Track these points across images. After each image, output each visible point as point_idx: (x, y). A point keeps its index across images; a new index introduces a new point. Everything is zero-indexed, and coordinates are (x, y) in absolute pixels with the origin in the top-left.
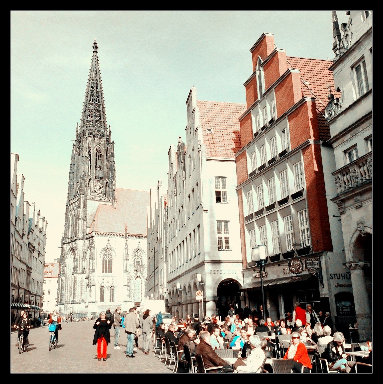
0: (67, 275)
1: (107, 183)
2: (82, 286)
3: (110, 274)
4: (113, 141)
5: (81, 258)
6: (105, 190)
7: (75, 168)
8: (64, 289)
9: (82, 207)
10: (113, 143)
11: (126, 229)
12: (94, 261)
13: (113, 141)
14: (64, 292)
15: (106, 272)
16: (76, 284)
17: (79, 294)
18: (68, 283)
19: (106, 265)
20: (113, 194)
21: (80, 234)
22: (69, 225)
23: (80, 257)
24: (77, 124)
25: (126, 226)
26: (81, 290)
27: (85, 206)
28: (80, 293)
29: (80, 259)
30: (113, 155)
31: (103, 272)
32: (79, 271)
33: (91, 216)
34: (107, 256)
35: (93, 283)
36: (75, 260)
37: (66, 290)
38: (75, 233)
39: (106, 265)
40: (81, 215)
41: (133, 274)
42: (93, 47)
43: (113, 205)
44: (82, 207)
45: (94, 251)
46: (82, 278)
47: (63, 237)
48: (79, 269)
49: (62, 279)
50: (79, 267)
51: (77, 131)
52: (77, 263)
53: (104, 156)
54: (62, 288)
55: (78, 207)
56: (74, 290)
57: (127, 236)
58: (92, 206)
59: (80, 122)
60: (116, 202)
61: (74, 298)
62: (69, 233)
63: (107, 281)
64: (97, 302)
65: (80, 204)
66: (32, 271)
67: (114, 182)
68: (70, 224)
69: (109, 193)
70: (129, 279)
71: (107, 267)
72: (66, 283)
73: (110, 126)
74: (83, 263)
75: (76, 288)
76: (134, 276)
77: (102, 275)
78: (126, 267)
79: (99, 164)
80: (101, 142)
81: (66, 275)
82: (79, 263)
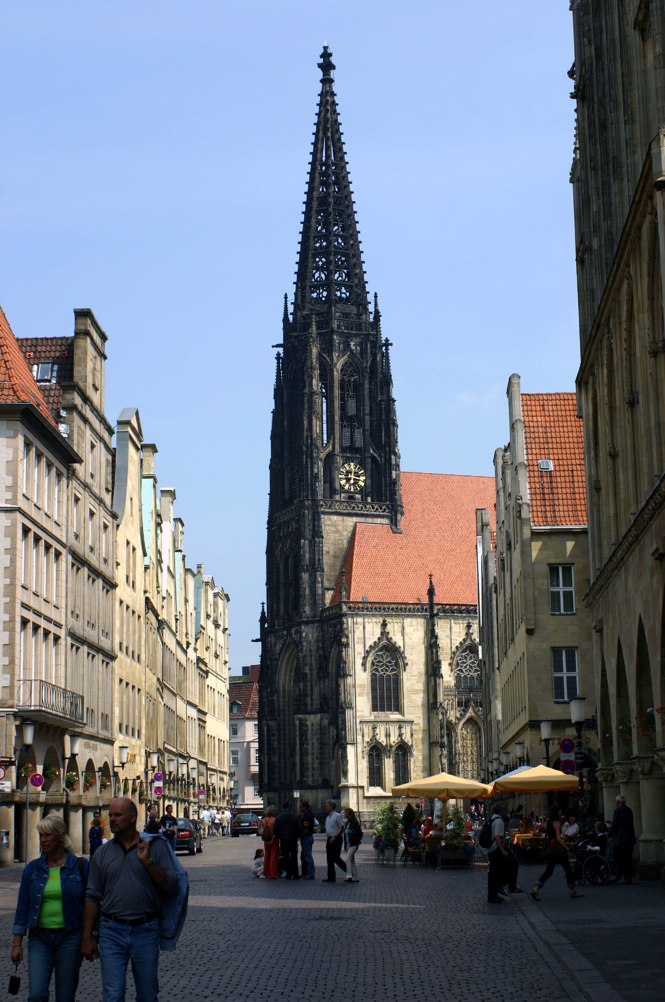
0: (282, 714)
2: (322, 744)
4: (387, 340)
5: (315, 672)
6: (369, 482)
7: (286, 423)
8: (276, 751)
9: (308, 533)
10: (387, 344)
11: (431, 592)
12: (349, 680)
13: (387, 340)
14: (275, 758)
15: (382, 710)
16: (306, 739)
17: (316, 766)
18: (284, 734)
19: (382, 689)
20: (393, 493)
22: (278, 582)
23: (311, 669)
24: (286, 297)
25: (431, 582)
26: (321, 753)
27: (317, 533)
28: (317, 761)
29: (311, 674)
30: (387, 381)
31: (374, 708)
32: (312, 704)
33: (334, 557)
34: (381, 666)
35: (349, 738)
36: (299, 676)
37: (280, 753)
38: (296, 603)
39: (382, 689)
40: (307, 556)
42: (320, 66)
43: (394, 522)
44: (308, 533)
45: (347, 655)
46: (320, 724)
47: (263, 613)
48: (312, 700)
49: (268, 725)
50: (312, 695)
52: (305, 686)
53: (363, 385)
54: (271, 749)
56: (301, 755)
57: (435, 612)
58: (335, 529)
59: (291, 290)
60: (402, 514)
61: (302, 776)
62: (278, 602)
64: (362, 787)
67: (393, 457)
68: (282, 581)
69: (383, 492)
71: (387, 695)
72: (279, 735)
73: (376, 296)
74: (322, 686)
75: (307, 749)
76: (456, 718)
77: (372, 718)
78: (435, 695)
80: (353, 348)
81: (279, 716)
82: (311, 685)
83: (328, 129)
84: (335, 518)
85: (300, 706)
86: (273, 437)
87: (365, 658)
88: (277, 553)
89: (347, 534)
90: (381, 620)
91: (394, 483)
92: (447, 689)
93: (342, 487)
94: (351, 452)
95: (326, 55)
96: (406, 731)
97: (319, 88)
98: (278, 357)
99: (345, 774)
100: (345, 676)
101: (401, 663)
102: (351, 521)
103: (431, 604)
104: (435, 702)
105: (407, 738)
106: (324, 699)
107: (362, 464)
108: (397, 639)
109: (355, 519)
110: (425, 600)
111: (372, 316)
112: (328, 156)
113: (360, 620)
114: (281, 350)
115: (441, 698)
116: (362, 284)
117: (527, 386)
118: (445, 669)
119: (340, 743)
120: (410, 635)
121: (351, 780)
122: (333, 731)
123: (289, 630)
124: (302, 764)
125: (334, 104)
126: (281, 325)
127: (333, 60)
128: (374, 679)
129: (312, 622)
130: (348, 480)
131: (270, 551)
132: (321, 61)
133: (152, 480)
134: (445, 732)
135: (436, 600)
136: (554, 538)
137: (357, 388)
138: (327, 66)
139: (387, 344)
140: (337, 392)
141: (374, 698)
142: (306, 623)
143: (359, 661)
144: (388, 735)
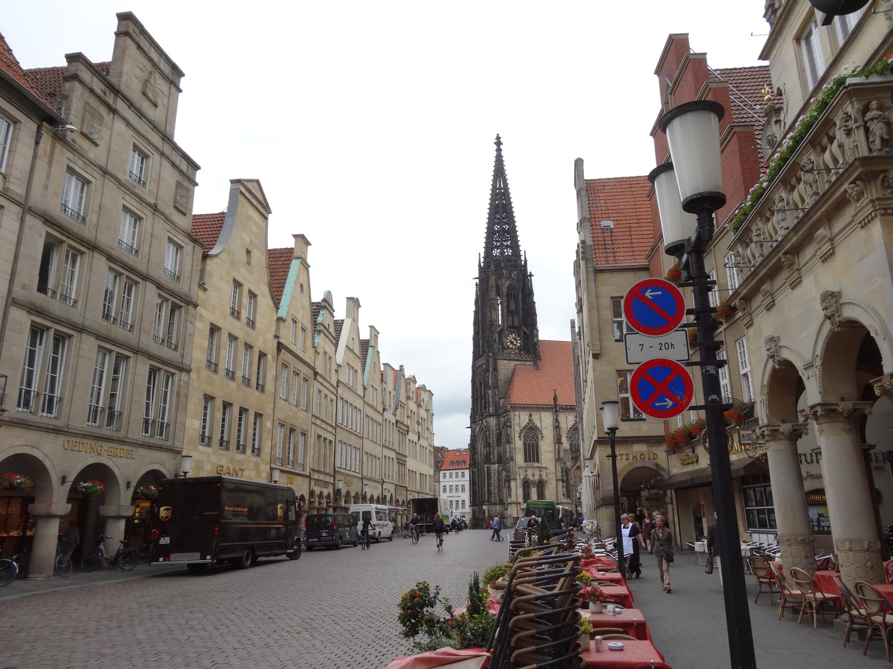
1: (525, 333)
2: (499, 480)
3: (536, 464)
10: (531, 275)
11: (555, 399)
12: (512, 446)
20: (536, 349)
21: (491, 409)
27: (495, 369)
30: (531, 293)
31: (526, 461)
35: (512, 477)
36: (488, 445)
41: (569, 464)
55: (487, 370)
58: (505, 367)
59: (482, 251)
63: (533, 475)
65: (488, 366)
66: (408, 459)
70: (566, 472)
71: (532, 454)
78: (559, 454)
79: (512, 307)
83: (499, 172)
84: (505, 362)
85: (488, 460)
88: (477, 381)
89: (511, 370)
90: (528, 413)
91: (536, 344)
92: (565, 450)
93: (508, 346)
94: (513, 328)
95: (498, 138)
96: (544, 473)
97: (495, 153)
98: (477, 285)
99: (510, 495)
101: (540, 436)
102: (513, 363)
103: (556, 406)
104: (559, 457)
105: (544, 477)
106: (500, 456)
107: (519, 335)
108: (538, 423)
109: (516, 362)
113: (517, 413)
114: (477, 281)
115: (562, 455)
117: (590, 174)
118: (564, 439)
119: (508, 480)
120: (544, 421)
121: (513, 499)
122: (504, 473)
123: (482, 420)
124: (488, 491)
127: (501, 140)
128: (525, 444)
129: (493, 416)
130: (512, 343)
131: (473, 381)
133: (299, 260)
134: (564, 473)
135: (558, 403)
136: (615, 274)
137: (516, 297)
138: (498, 143)
139: (531, 275)
140: (505, 299)
141: (525, 456)
142: (490, 416)
143: (517, 435)
144: (533, 475)
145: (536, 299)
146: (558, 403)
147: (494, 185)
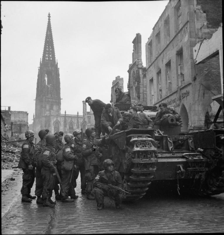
10: (59, 69)
12: (51, 127)
24: (41, 59)
30: (58, 75)
42: (48, 16)
51: (40, 63)
59: (42, 57)
86: (37, 83)
87: (53, 123)
95: (49, 14)
97: (48, 20)
98: (39, 69)
100: (50, 126)
108: (59, 120)
110: (64, 114)
111: (56, 64)
112: (49, 34)
114: (39, 68)
116: (55, 58)
125: (50, 24)
126: (39, 63)
127: (51, 15)
132: (48, 15)
135: (66, 114)
138: (49, 16)
143: (52, 124)
145: (60, 77)
146: (66, 114)
147: (47, 33)
